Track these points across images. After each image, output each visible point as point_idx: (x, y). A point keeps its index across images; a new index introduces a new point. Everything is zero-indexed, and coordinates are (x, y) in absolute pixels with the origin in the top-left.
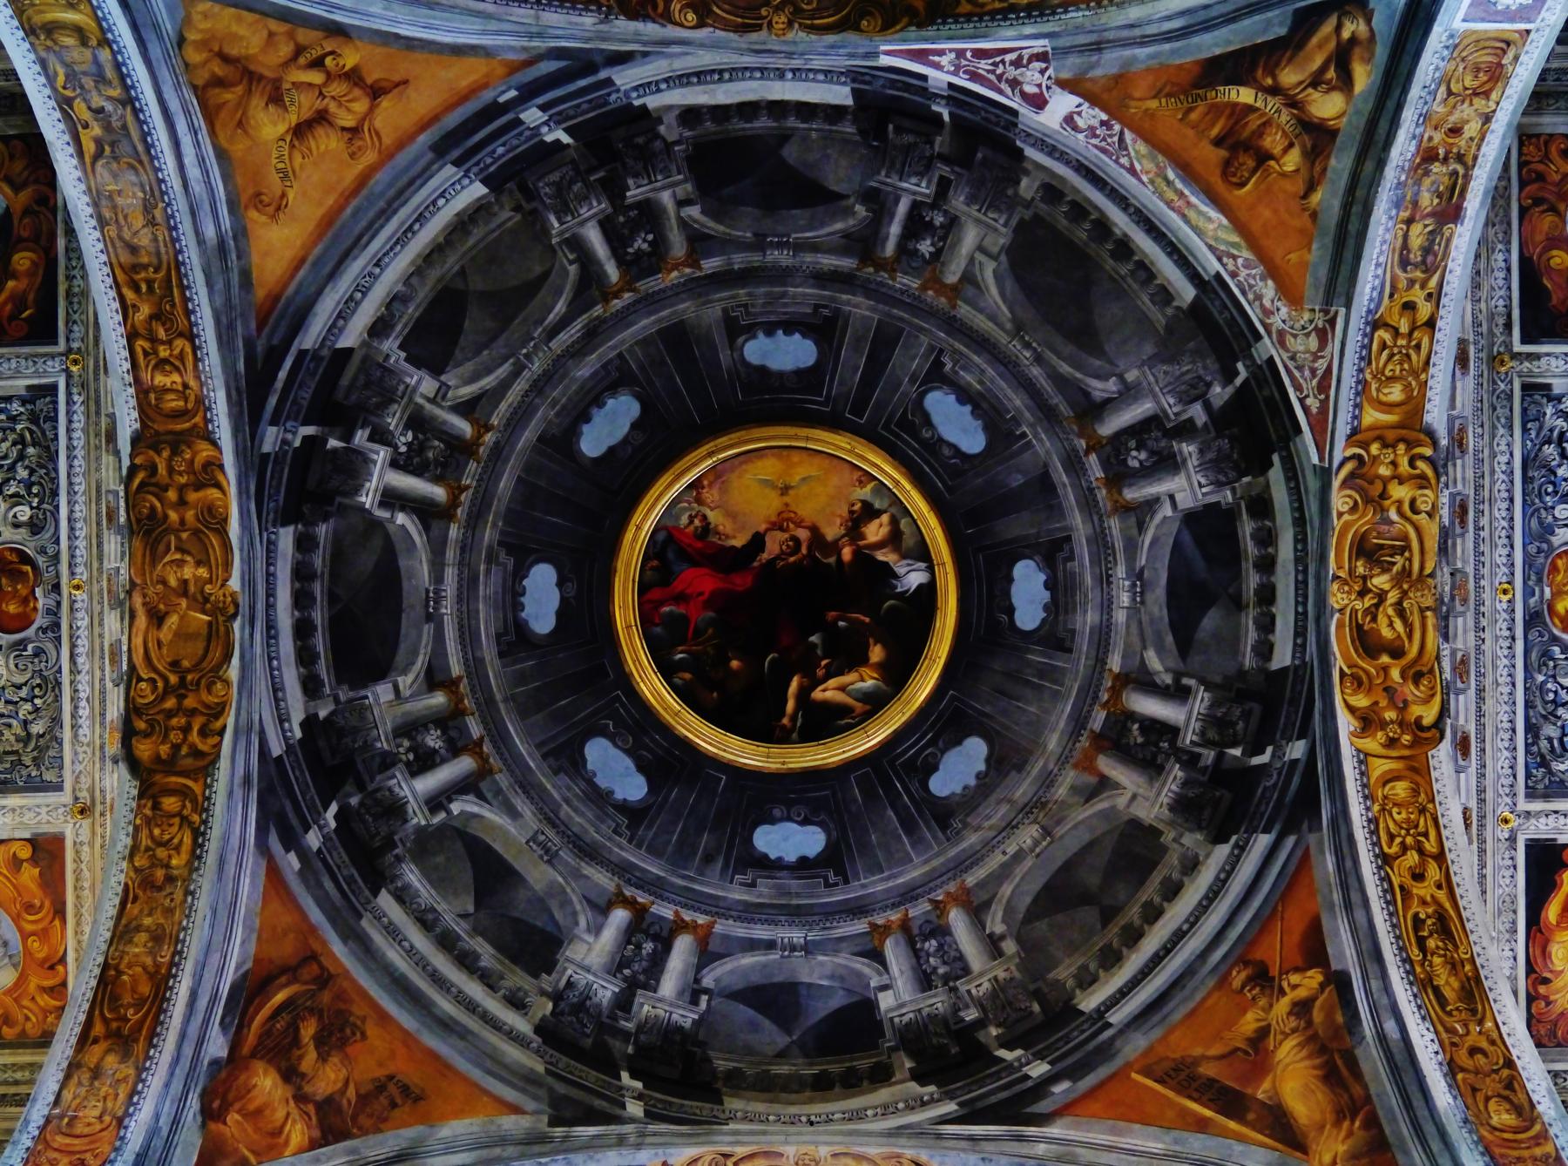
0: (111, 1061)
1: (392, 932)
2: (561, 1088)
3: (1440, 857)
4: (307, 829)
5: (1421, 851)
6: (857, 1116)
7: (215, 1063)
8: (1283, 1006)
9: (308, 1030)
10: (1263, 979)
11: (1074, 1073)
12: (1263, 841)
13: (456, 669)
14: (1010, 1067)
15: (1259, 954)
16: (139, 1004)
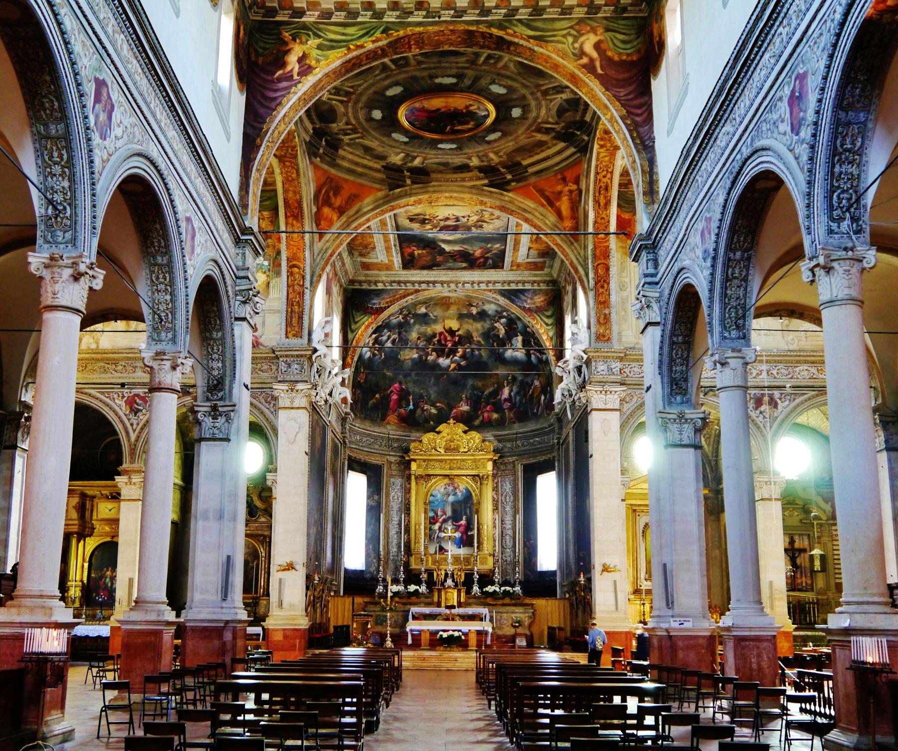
0: (295, 222)
1: (344, 158)
2: (390, 181)
3: (612, 173)
4: (319, 149)
5: (607, 171)
6: (463, 180)
7: (316, 213)
8: (567, 188)
9: (331, 194)
10: (564, 180)
11: (518, 181)
12: (572, 150)
13: (354, 122)
14: (502, 174)
15: (566, 174)
16: (296, 208)
